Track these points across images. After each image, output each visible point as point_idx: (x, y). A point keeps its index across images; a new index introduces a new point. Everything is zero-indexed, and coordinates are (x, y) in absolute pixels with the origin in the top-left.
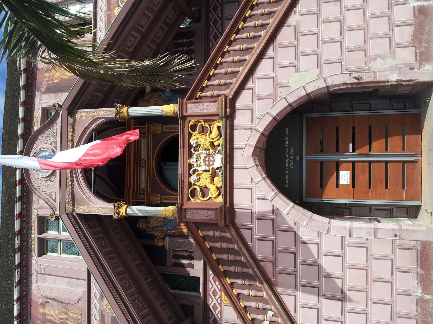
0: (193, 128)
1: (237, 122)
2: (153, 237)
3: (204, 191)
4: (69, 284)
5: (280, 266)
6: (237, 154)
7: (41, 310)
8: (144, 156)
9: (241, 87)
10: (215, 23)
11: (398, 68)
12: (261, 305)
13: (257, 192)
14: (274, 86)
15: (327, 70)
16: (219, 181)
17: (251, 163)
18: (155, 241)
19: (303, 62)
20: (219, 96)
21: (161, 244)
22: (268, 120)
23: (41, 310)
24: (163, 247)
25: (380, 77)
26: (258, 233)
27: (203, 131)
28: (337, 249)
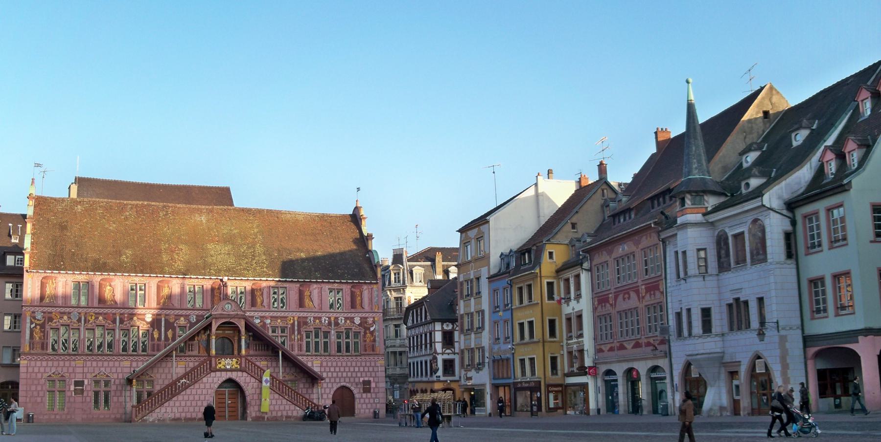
0: (238, 360)
1: (238, 372)
2: (198, 336)
3: (220, 363)
4: (178, 300)
5: (201, 384)
6: (230, 373)
7: (166, 285)
8: (226, 332)
9: (248, 374)
10: (271, 359)
11: (251, 412)
12: (190, 379)
13: (220, 378)
14: (248, 383)
15: (251, 396)
16: (223, 367)
17: (228, 377)
18: (197, 337)
19: (254, 390)
20: (246, 367)
21: (196, 339)
22: (239, 381)
23: (166, 285)
24: (195, 340)
25: (249, 409)
26: (209, 379)
27: (237, 362)
28: (206, 399)
